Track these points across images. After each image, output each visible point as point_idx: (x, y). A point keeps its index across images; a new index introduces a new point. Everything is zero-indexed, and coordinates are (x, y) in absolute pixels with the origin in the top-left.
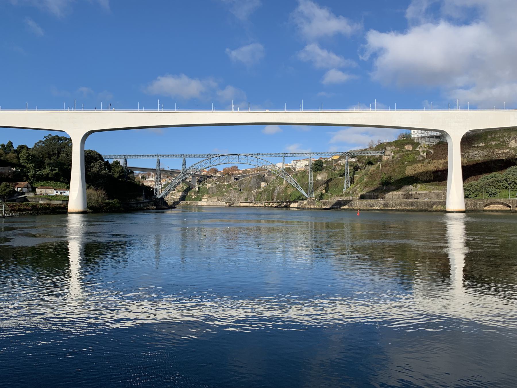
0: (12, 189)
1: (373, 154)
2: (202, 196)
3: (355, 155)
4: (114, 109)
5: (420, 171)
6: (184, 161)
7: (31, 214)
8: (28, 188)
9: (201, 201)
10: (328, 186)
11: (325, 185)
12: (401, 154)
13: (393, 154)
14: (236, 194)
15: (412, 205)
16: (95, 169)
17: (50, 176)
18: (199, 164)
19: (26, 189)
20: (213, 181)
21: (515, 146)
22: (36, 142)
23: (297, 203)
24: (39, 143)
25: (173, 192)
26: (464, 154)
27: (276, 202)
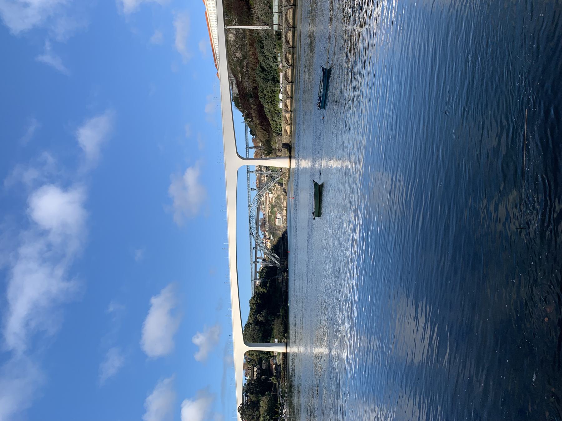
7: (287, 372)
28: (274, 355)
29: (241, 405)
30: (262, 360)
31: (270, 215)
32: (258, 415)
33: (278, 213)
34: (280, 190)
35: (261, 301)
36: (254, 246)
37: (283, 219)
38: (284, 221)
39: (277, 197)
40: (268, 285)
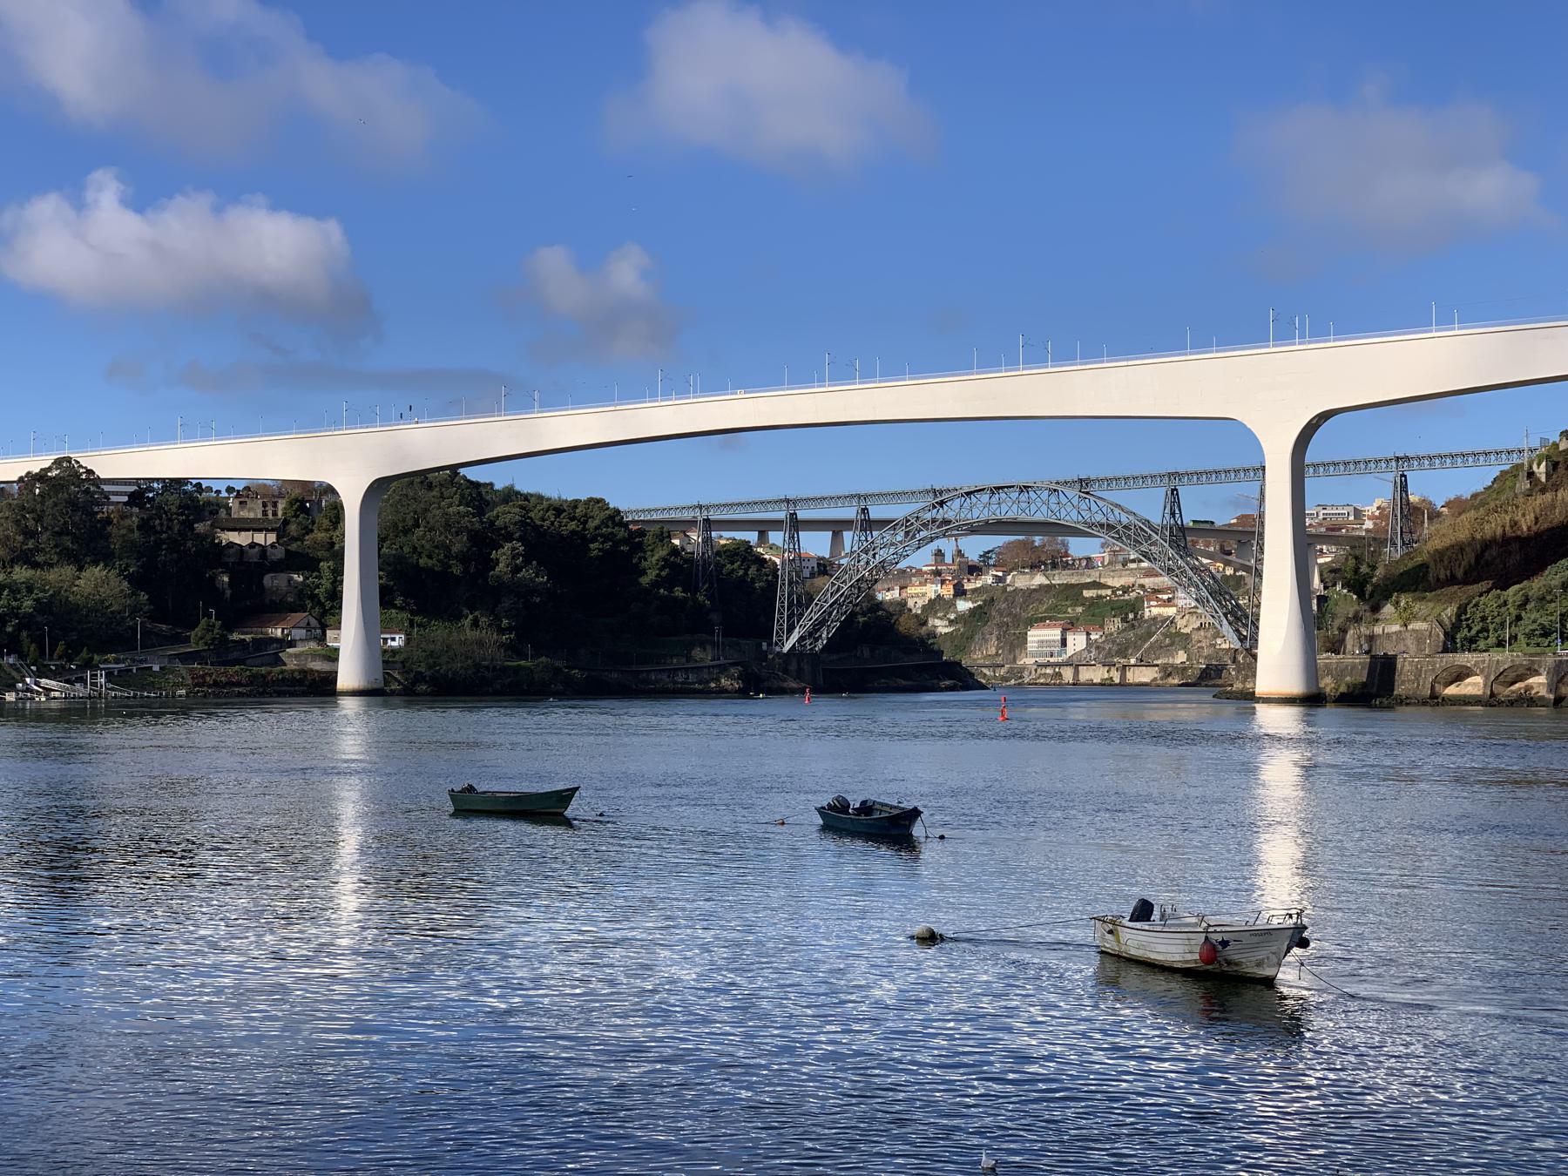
7: (240, 694)
8: (308, 627)
28: (329, 633)
29: (90, 472)
31: (1087, 594)
32: (40, 558)
33: (1093, 637)
34: (1214, 645)
35: (597, 557)
36: (876, 513)
37: (1059, 665)
38: (1049, 671)
39: (1179, 634)
40: (678, 592)
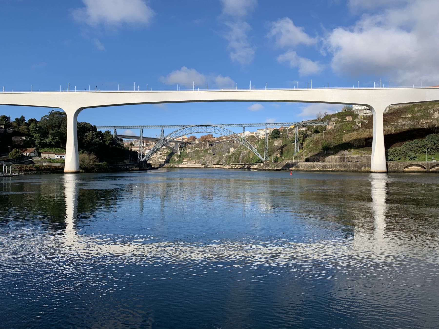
0: (20, 154)
1: (321, 124)
2: (183, 159)
3: (306, 125)
4: (99, 90)
5: (354, 139)
6: (162, 131)
7: (35, 174)
8: (35, 153)
9: (182, 164)
10: (282, 151)
11: (280, 150)
12: (341, 124)
13: (335, 124)
14: (210, 158)
15: (345, 166)
16: (88, 138)
17: (52, 143)
18: (174, 133)
19: (34, 154)
20: (192, 147)
21: (438, 117)
22: (42, 117)
23: (256, 165)
24: (45, 117)
25: (160, 156)
26: (394, 124)
27: (240, 164)
28: (43, 155)
30: (27, 137)
